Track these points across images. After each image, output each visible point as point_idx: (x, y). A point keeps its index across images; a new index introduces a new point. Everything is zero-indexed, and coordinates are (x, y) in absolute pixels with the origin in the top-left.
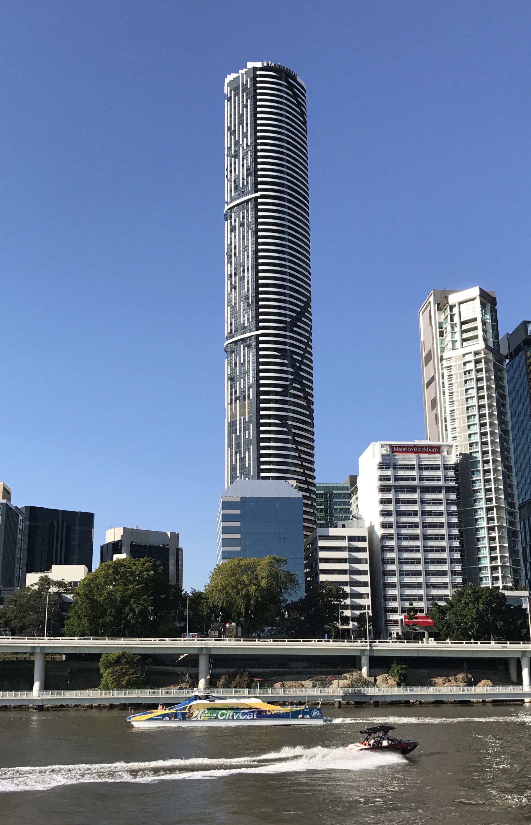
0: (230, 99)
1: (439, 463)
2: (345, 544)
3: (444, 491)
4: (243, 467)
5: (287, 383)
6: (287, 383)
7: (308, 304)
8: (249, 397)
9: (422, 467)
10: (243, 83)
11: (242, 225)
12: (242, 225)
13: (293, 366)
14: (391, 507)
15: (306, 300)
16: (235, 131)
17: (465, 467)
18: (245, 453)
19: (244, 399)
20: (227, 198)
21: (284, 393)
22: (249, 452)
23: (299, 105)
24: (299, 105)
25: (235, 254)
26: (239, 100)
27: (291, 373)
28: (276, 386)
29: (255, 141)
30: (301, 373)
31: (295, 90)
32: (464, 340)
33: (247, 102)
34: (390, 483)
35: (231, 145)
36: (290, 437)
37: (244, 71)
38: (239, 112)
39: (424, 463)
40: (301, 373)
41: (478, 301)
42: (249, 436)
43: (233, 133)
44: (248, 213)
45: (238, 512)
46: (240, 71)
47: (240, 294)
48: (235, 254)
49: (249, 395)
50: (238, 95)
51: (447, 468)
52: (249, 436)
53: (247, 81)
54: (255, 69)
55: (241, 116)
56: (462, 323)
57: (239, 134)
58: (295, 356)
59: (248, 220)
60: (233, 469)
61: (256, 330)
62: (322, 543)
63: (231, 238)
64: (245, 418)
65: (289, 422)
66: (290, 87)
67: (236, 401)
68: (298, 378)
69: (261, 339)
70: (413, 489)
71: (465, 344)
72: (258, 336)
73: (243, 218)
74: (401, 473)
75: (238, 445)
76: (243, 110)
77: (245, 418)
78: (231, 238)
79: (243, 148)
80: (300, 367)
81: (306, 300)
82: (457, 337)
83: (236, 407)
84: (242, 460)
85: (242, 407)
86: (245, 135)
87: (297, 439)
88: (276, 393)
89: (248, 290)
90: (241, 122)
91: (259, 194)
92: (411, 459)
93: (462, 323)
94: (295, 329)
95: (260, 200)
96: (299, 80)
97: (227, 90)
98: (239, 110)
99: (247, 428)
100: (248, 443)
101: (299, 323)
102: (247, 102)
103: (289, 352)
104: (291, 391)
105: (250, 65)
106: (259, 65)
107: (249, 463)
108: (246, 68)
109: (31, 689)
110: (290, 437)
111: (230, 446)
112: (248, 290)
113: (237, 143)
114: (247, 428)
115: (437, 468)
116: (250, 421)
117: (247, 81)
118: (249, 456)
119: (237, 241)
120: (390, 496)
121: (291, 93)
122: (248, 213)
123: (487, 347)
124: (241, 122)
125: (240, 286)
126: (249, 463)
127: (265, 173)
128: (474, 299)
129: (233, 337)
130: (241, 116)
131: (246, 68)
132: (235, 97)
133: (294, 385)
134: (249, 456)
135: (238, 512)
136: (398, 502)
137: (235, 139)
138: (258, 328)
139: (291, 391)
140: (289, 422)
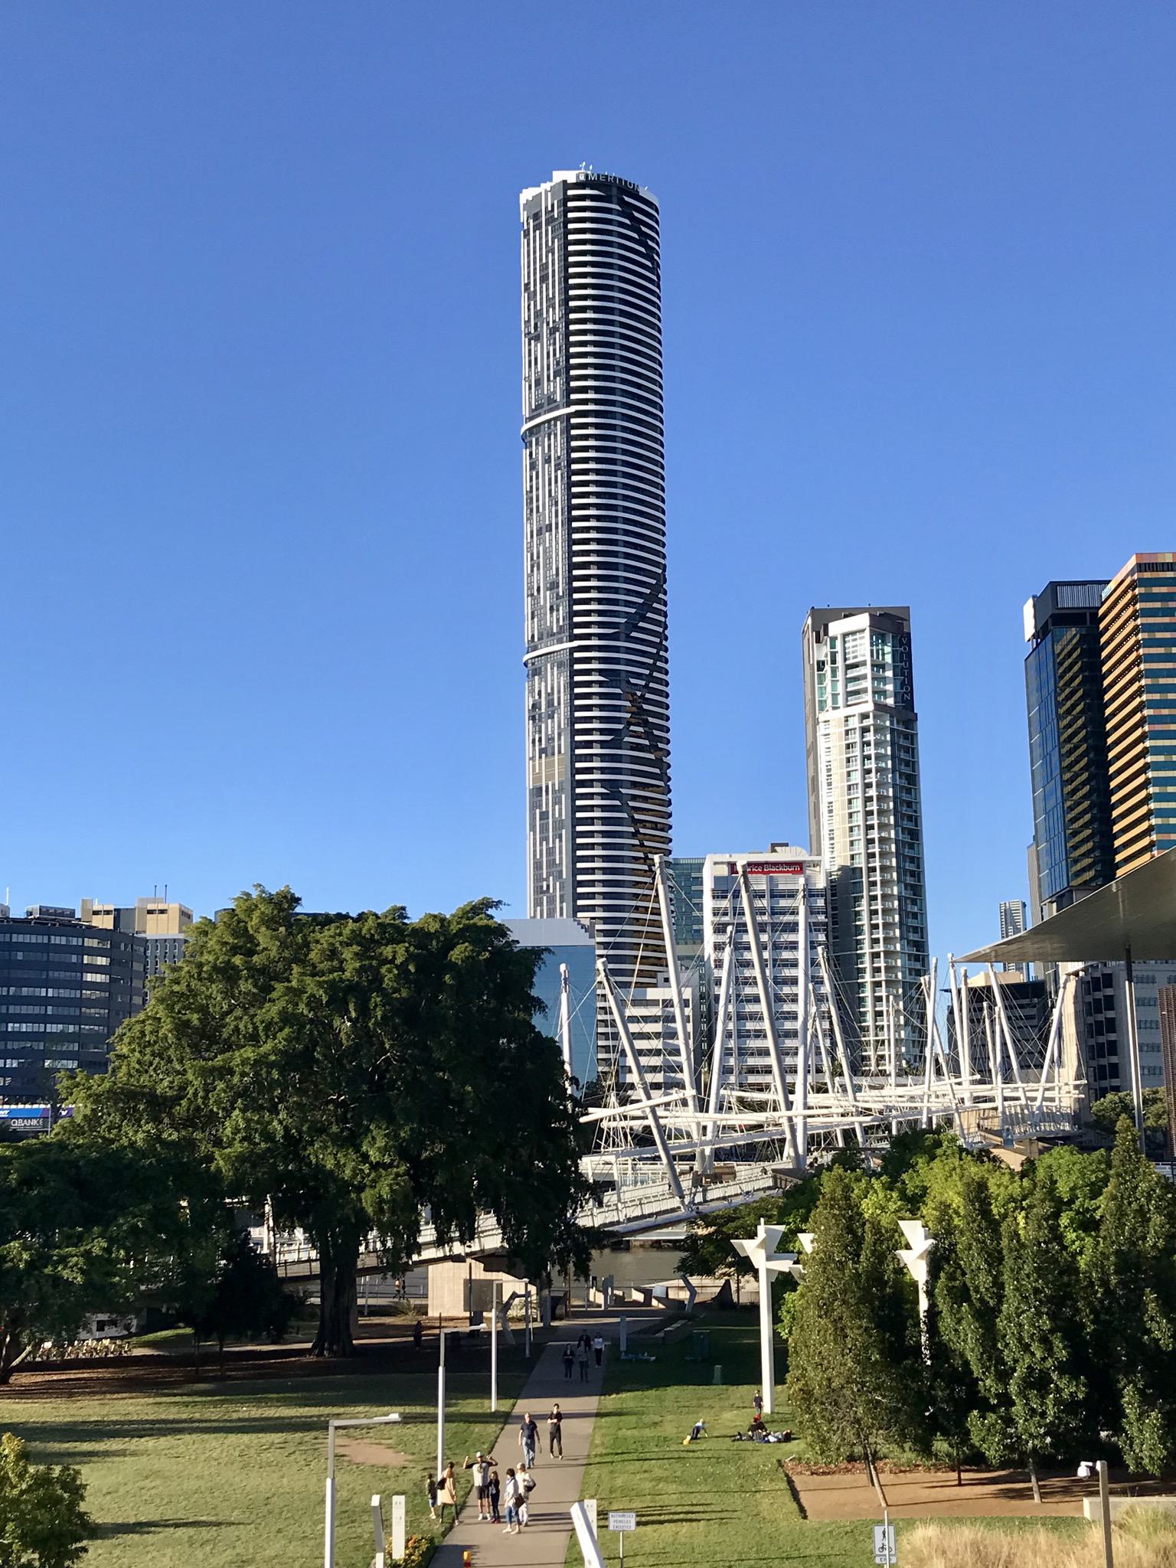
0: (527, 234)
4: (551, 863)
5: (621, 727)
6: (621, 727)
7: (659, 588)
11: (548, 461)
12: (548, 461)
15: (654, 582)
16: (535, 291)
17: (843, 891)
20: (526, 412)
21: (615, 744)
22: (560, 837)
23: (643, 240)
24: (643, 240)
28: (602, 732)
29: (567, 314)
30: (645, 707)
31: (637, 215)
32: (850, 694)
36: (625, 815)
37: (547, 186)
39: (781, 887)
40: (645, 707)
41: (867, 633)
47: (545, 577)
50: (540, 228)
51: (810, 894)
54: (566, 185)
56: (849, 667)
58: (633, 681)
60: (538, 866)
61: (571, 641)
65: (623, 791)
66: (627, 210)
68: (639, 715)
71: (852, 700)
72: (573, 650)
75: (544, 829)
80: (642, 696)
81: (654, 582)
82: (840, 689)
84: (551, 852)
85: (550, 766)
87: (637, 816)
88: (603, 744)
90: (544, 279)
91: (573, 409)
93: (849, 667)
94: (634, 634)
96: (644, 192)
99: (557, 801)
100: (559, 825)
101: (649, 615)
103: (623, 675)
104: (626, 739)
105: (559, 176)
106: (571, 177)
107: (561, 859)
108: (551, 180)
110: (625, 815)
111: (533, 828)
113: (538, 314)
114: (557, 801)
116: (561, 790)
118: (561, 847)
119: (541, 484)
121: (627, 222)
123: (880, 708)
124: (544, 279)
126: (561, 859)
127: (585, 374)
128: (863, 631)
129: (535, 649)
131: (551, 180)
133: (632, 728)
134: (561, 847)
138: (573, 638)
139: (626, 739)
140: (623, 791)
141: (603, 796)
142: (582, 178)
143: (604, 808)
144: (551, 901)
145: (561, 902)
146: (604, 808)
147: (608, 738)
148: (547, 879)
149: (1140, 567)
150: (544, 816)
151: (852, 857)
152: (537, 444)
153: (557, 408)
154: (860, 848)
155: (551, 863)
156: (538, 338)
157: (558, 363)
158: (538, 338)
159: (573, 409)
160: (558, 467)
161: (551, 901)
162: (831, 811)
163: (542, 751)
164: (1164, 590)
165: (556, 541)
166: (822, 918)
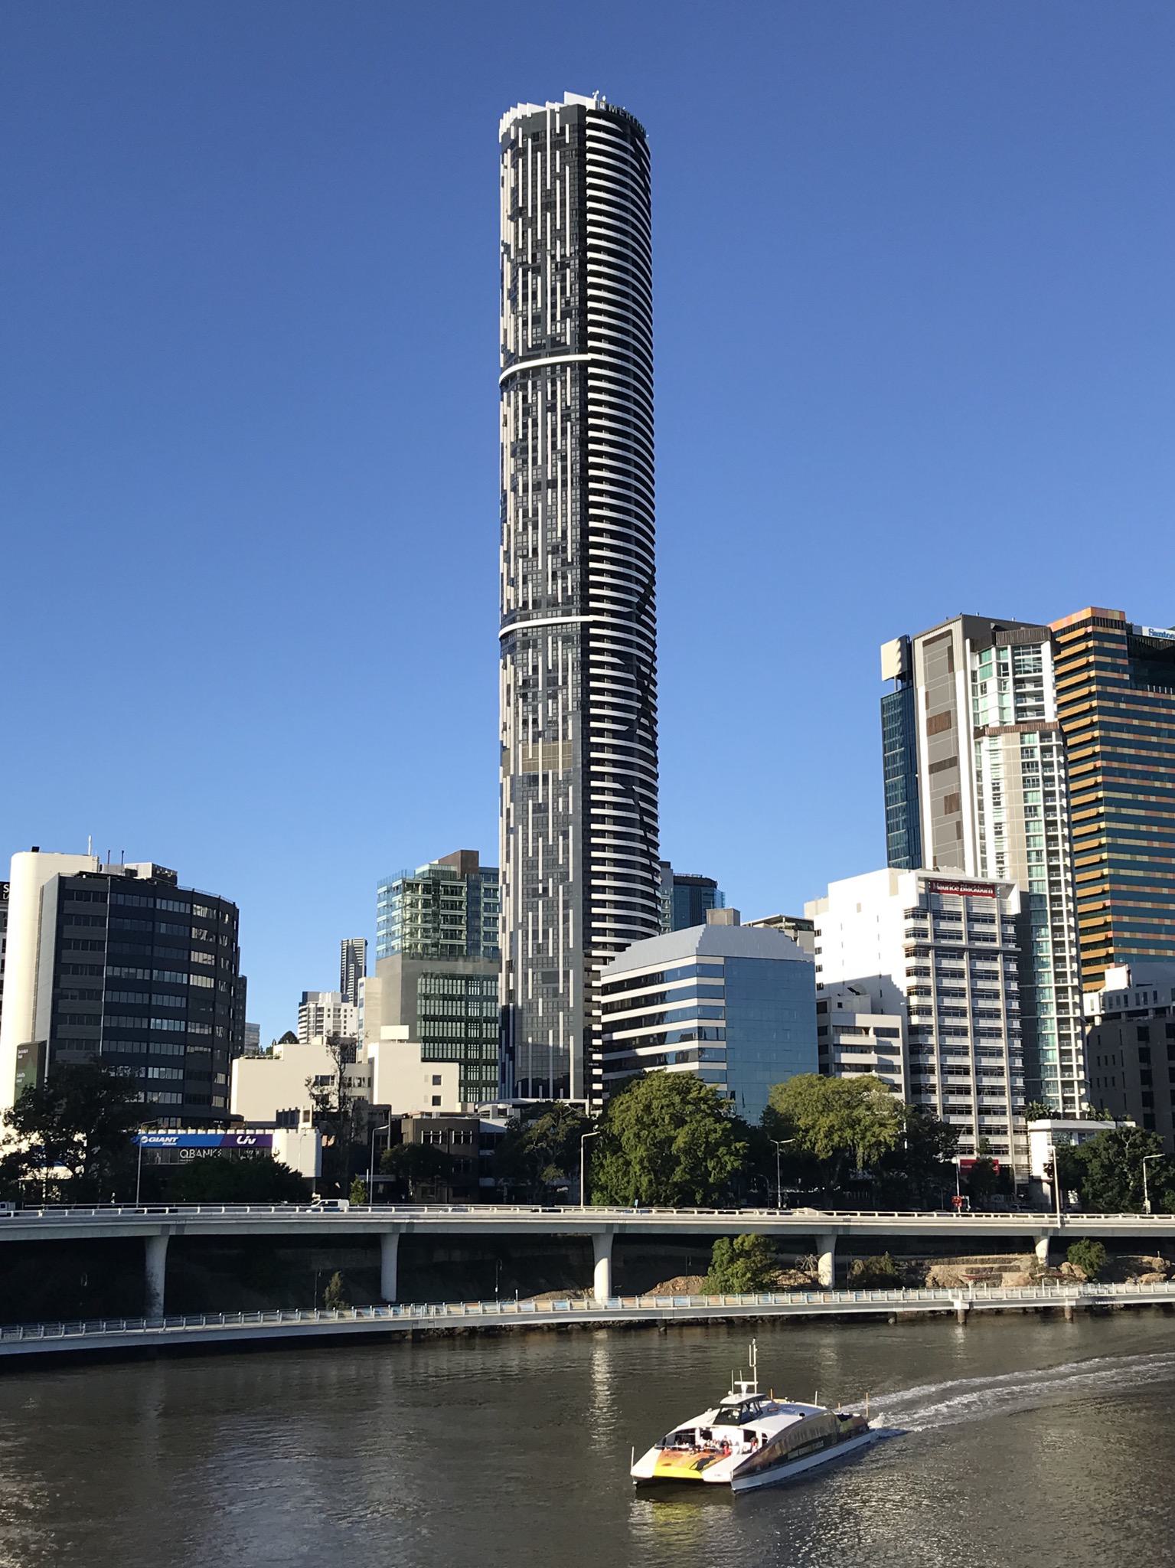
1: (995, 911)
2: (871, 1040)
3: (1000, 957)
4: (551, 863)
5: (634, 717)
6: (634, 717)
9: (972, 918)
10: (553, 128)
11: (553, 408)
18: (555, 839)
19: (556, 739)
22: (566, 836)
25: (535, 460)
26: (544, 161)
27: (639, 699)
28: (614, 720)
33: (563, 169)
34: (929, 940)
35: (525, 243)
37: (557, 106)
38: (544, 184)
39: (975, 910)
42: (566, 807)
43: (528, 222)
44: (564, 387)
45: (721, 982)
46: (549, 106)
48: (535, 460)
50: (544, 150)
51: (1005, 920)
52: (566, 807)
53: (563, 129)
55: (549, 195)
57: (544, 227)
59: (564, 400)
60: (530, 865)
62: (845, 1039)
63: (525, 426)
64: (555, 774)
67: (535, 741)
69: (593, 631)
70: (958, 953)
72: (586, 626)
73: (554, 393)
74: (944, 925)
76: (553, 183)
77: (555, 774)
78: (525, 426)
79: (553, 257)
86: (558, 235)
88: (615, 734)
89: (564, 532)
90: (549, 206)
91: (589, 357)
92: (955, 904)
95: (591, 370)
98: (544, 179)
99: (560, 792)
100: (562, 822)
102: (563, 169)
105: (571, 99)
106: (590, 104)
109: (588, 1282)
112: (564, 532)
115: (989, 919)
116: (567, 781)
117: (563, 129)
120: (929, 962)
122: (564, 387)
124: (549, 206)
125: (544, 525)
130: (549, 195)
131: (562, 101)
132: (534, 152)
135: (721, 982)
136: (941, 973)
137: (535, 234)
141: (615, 792)
142: (603, 107)
143: (616, 806)
144: (550, 907)
145: (566, 907)
146: (616, 806)
148: (545, 880)
149: (1094, 620)
151: (1030, 883)
152: (534, 387)
153: (567, 353)
155: (551, 863)
156: (538, 270)
157: (567, 303)
158: (538, 270)
159: (589, 357)
160: (566, 418)
161: (550, 907)
162: (998, 833)
163: (537, 736)
164: (1113, 646)
165: (564, 504)
166: (1012, 946)
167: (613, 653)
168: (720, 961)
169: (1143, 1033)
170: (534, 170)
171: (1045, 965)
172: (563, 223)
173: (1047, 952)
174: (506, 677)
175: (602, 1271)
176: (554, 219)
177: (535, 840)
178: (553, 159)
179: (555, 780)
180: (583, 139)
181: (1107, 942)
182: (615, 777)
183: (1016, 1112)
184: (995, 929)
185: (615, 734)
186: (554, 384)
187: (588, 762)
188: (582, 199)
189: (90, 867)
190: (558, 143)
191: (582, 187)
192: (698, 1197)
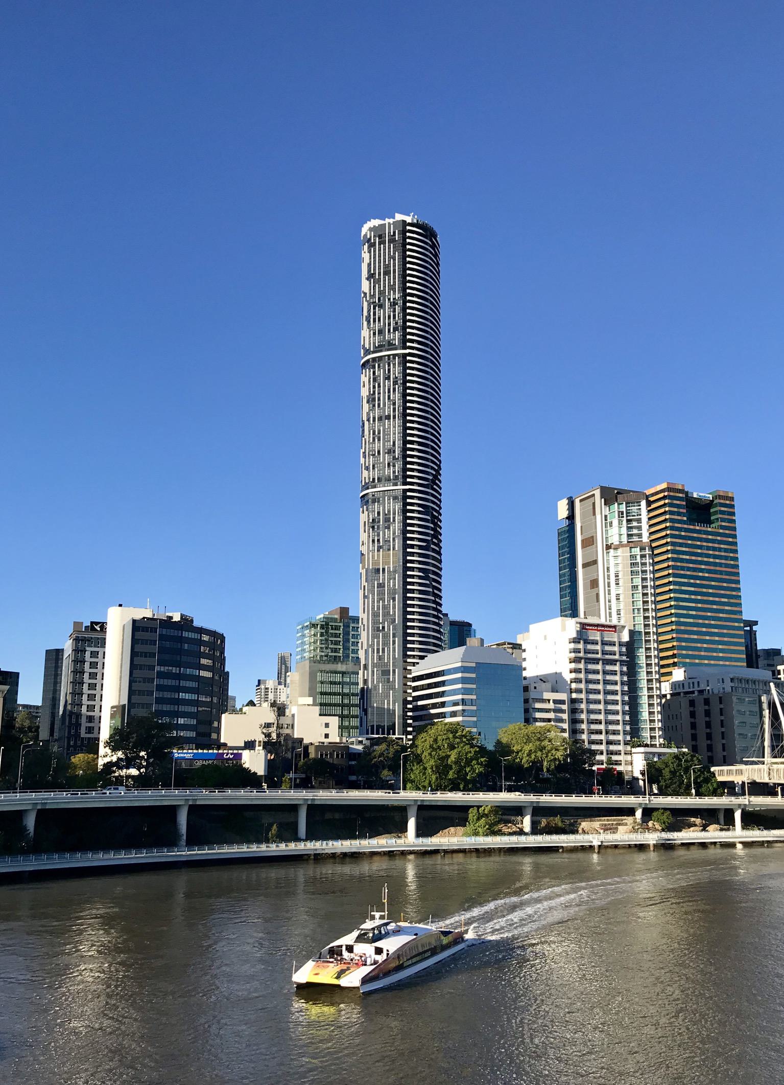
1: (616, 640)
2: (551, 706)
3: (618, 664)
4: (386, 614)
5: (429, 538)
6: (429, 538)
8: (394, 549)
9: (604, 643)
10: (389, 232)
11: (388, 378)
13: (433, 523)
14: (582, 676)
19: (389, 550)
22: (394, 599)
26: (385, 249)
27: (432, 529)
33: (394, 253)
34: (582, 655)
35: (374, 292)
37: (391, 221)
38: (385, 261)
39: (606, 639)
45: (474, 675)
46: (387, 221)
49: (394, 545)
51: (621, 644)
53: (394, 233)
55: (387, 267)
57: (385, 284)
60: (376, 615)
63: (374, 387)
67: (378, 551)
69: (408, 494)
70: (596, 661)
72: (405, 491)
73: (389, 370)
74: (589, 647)
76: (389, 261)
77: (389, 568)
78: (374, 387)
79: (389, 299)
83: (378, 556)
85: (386, 557)
86: (392, 288)
88: (420, 547)
89: (394, 443)
90: (387, 273)
91: (408, 351)
92: (596, 636)
95: (408, 358)
97: (365, 229)
98: (385, 259)
100: (392, 593)
102: (394, 253)
105: (399, 217)
106: (409, 219)
109: (403, 829)
112: (394, 443)
113: (382, 293)
116: (395, 571)
117: (394, 233)
120: (581, 666)
124: (387, 273)
125: (384, 438)
127: (413, 332)
130: (387, 267)
132: (380, 244)
135: (474, 675)
136: (588, 671)
137: (379, 287)
138: (405, 483)
142: (415, 221)
143: (420, 584)
144: (386, 636)
145: (394, 636)
146: (420, 584)
147: (424, 544)
148: (383, 622)
149: (669, 489)
150: (381, 586)
152: (379, 367)
153: (396, 349)
154: (640, 620)
155: (386, 614)
156: (381, 306)
157: (396, 323)
158: (381, 306)
159: (408, 351)
160: (395, 383)
161: (386, 636)
162: (618, 599)
163: (379, 548)
164: (678, 502)
165: (394, 429)
166: (624, 658)
167: (419, 505)
168: (474, 665)
169: (692, 703)
170: (380, 254)
171: (641, 667)
172: (394, 282)
173: (642, 661)
174: (363, 517)
175: (412, 824)
176: (389, 280)
177: (378, 602)
178: (389, 248)
179: (389, 571)
180: (405, 238)
181: (674, 656)
182: (420, 570)
183: (626, 743)
184: (616, 649)
185: (420, 547)
186: (389, 365)
187: (406, 561)
188: (405, 269)
189: (149, 615)
190: (392, 240)
191: (405, 263)
192: (461, 786)
